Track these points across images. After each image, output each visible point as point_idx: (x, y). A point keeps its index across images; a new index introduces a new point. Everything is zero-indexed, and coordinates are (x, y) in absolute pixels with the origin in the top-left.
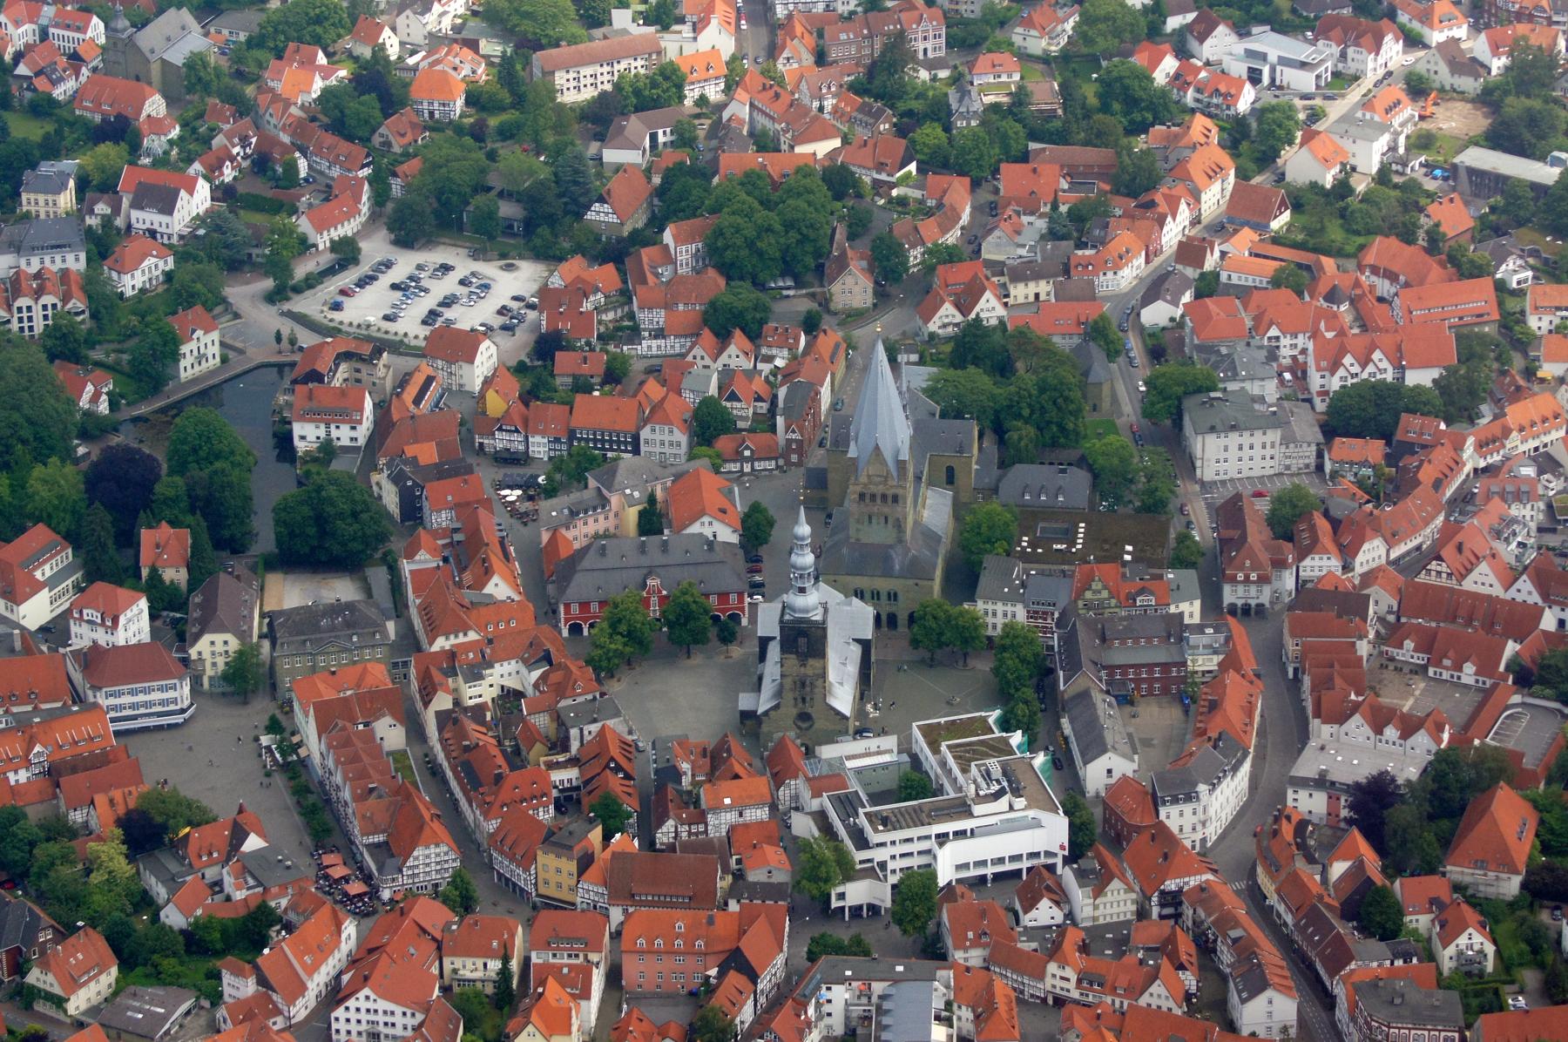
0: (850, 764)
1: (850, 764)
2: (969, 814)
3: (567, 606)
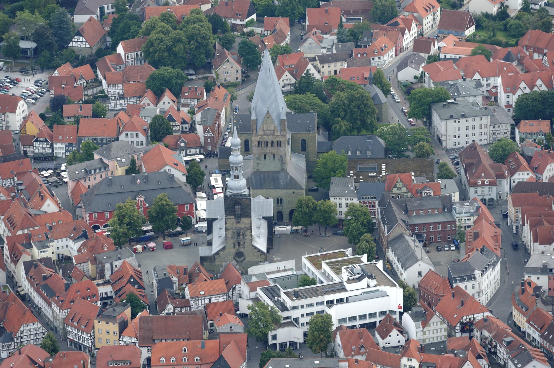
0: (269, 276)
1: (269, 276)
2: (344, 290)
3: (91, 215)
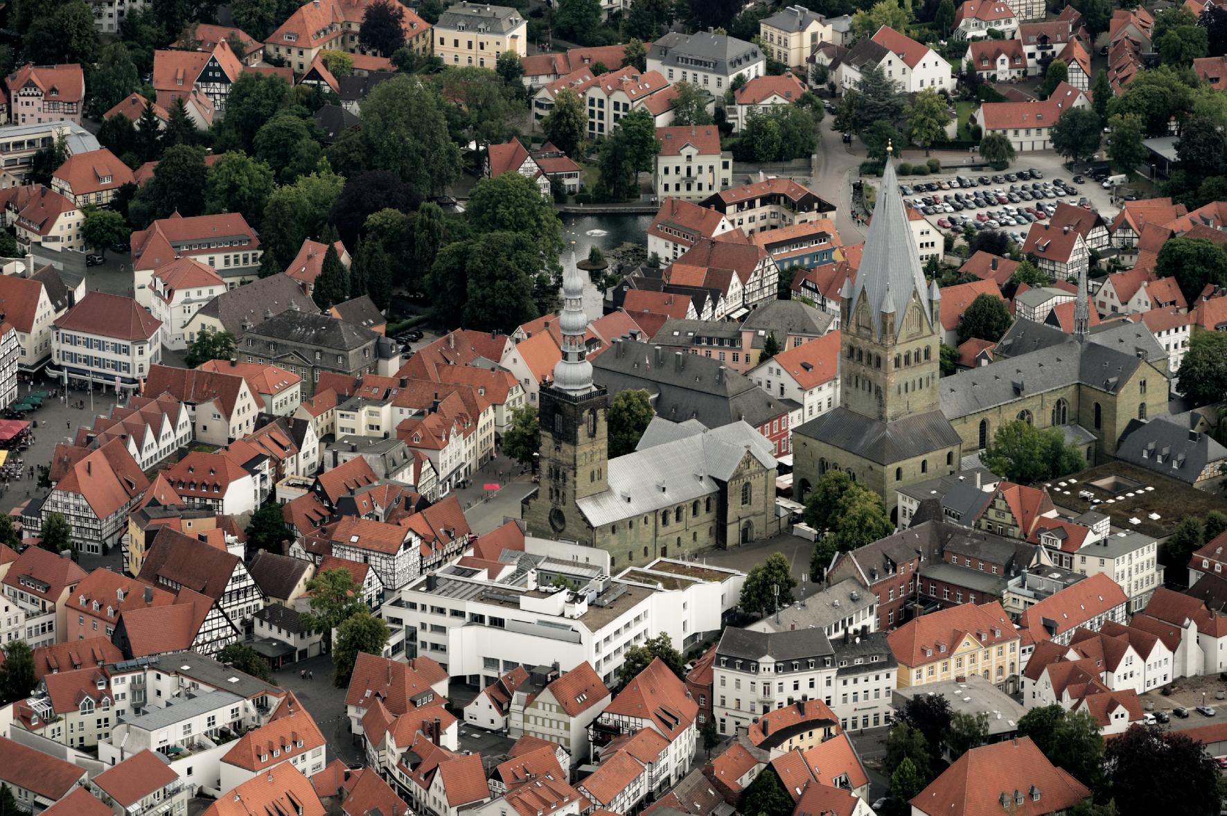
2: (516, 605)
